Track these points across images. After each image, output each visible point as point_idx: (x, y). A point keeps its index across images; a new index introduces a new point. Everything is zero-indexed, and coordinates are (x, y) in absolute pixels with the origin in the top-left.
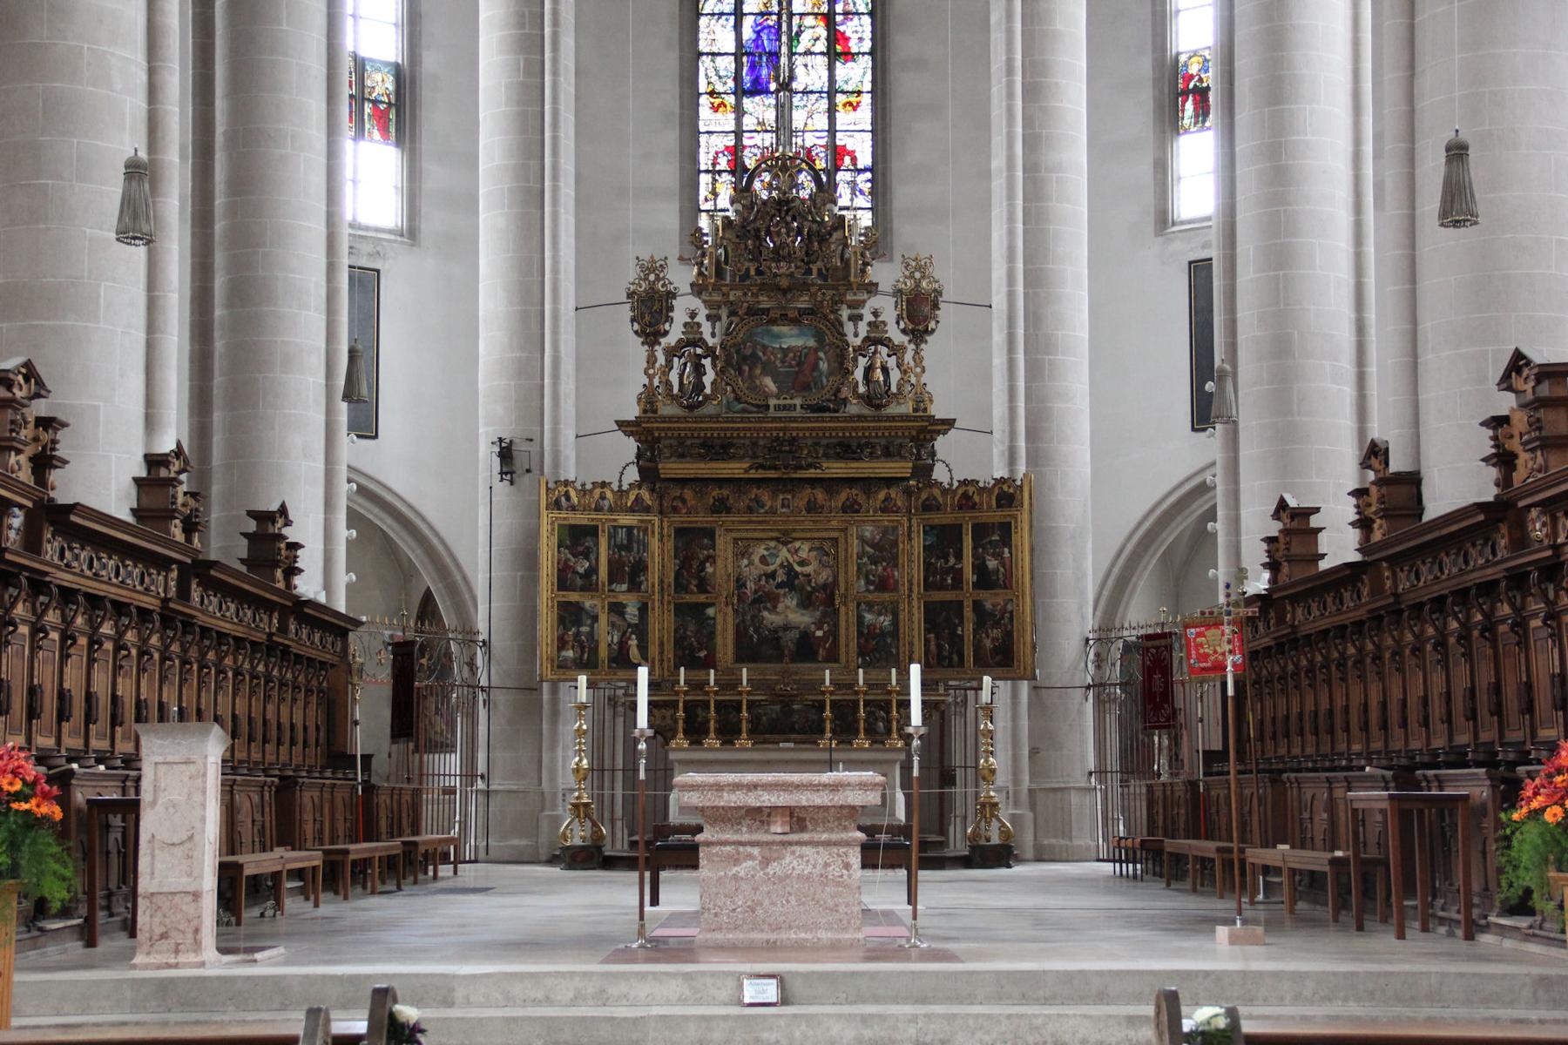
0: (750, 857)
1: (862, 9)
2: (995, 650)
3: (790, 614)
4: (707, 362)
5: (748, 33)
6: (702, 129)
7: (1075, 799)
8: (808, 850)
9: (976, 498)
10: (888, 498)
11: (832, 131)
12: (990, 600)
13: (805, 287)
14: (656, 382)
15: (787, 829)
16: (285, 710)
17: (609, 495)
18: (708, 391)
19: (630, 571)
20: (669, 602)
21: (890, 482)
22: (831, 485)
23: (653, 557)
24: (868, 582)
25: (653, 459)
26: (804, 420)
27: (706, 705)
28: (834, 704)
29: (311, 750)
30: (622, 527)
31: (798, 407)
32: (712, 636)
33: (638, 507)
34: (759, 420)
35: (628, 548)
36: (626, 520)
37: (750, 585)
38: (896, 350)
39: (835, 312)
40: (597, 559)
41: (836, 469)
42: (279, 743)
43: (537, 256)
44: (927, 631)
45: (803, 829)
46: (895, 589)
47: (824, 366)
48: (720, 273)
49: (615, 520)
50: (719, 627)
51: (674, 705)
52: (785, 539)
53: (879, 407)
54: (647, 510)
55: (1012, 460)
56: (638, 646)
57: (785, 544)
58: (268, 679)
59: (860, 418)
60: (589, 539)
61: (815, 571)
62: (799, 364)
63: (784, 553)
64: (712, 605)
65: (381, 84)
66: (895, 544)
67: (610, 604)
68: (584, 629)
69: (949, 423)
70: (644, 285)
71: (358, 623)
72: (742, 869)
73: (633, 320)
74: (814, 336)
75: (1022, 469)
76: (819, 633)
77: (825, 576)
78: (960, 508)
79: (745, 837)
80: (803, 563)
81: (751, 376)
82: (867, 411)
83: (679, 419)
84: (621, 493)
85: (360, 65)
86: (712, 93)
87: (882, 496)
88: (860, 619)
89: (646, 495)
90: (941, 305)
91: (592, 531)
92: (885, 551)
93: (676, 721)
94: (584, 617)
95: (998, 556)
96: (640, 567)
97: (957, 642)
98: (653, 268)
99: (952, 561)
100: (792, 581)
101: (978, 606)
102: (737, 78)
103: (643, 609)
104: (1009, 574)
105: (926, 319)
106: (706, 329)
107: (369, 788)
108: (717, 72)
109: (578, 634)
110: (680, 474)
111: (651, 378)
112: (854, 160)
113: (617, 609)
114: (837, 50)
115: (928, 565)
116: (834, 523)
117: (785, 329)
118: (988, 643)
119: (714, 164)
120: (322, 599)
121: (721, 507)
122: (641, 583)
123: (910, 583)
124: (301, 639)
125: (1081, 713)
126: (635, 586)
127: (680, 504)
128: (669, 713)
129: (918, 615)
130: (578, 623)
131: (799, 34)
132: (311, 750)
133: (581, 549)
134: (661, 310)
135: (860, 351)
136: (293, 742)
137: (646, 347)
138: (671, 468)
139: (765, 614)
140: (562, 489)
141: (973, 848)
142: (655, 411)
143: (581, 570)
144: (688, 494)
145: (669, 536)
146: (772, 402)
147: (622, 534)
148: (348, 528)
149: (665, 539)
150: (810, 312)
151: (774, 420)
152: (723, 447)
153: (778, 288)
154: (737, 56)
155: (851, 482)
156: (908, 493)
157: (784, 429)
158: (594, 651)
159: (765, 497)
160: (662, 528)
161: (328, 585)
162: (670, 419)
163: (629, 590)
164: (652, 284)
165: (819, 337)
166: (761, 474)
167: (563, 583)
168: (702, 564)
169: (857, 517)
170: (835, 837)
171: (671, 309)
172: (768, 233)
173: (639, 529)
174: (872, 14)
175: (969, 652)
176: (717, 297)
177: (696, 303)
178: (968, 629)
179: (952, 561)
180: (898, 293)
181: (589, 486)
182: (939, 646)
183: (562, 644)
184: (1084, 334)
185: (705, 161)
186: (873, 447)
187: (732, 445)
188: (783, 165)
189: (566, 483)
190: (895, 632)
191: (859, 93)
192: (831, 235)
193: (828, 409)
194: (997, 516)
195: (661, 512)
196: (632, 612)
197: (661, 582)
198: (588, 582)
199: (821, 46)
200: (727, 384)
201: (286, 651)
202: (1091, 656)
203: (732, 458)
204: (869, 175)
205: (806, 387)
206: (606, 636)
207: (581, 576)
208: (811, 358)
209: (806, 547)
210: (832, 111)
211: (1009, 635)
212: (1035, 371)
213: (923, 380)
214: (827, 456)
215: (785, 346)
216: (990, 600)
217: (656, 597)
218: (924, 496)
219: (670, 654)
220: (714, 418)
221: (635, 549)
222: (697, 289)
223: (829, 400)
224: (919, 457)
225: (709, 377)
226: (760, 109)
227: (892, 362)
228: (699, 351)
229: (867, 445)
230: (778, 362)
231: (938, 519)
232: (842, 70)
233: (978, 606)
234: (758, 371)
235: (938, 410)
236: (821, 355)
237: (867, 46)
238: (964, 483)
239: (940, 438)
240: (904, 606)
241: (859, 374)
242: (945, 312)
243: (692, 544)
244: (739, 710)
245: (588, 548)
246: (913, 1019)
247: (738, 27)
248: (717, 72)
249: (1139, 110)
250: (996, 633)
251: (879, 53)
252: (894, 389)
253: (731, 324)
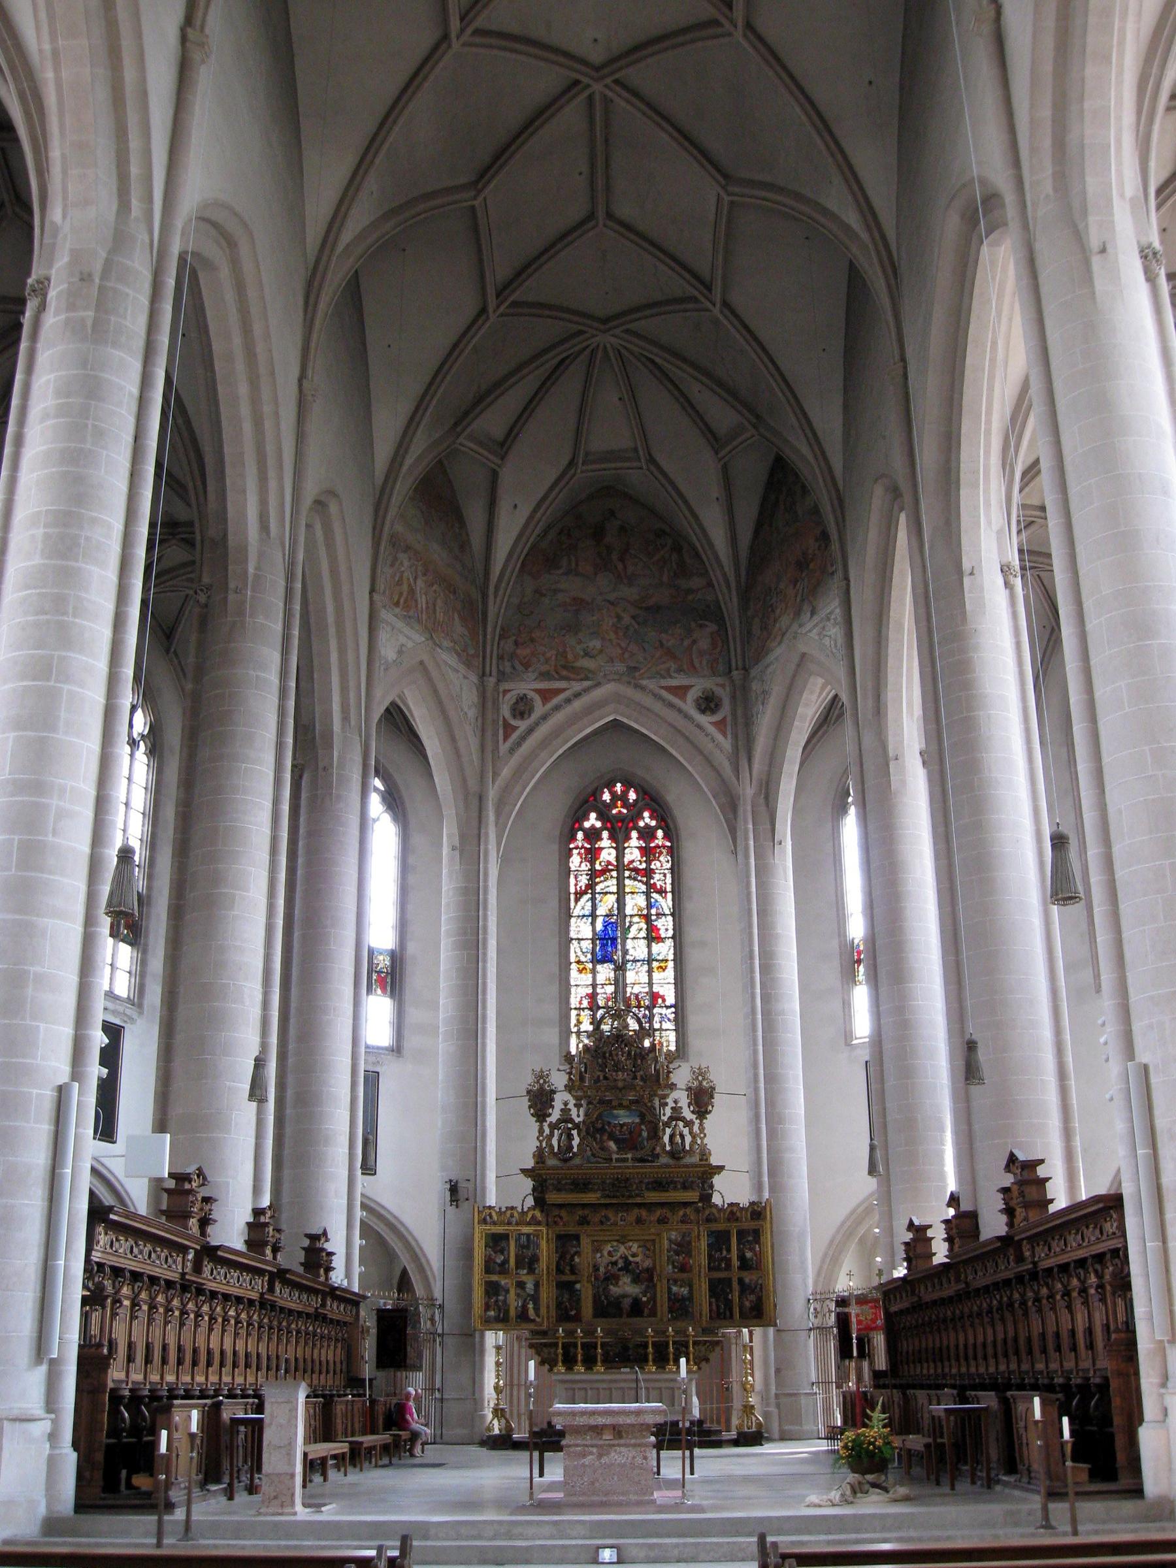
0: (591, 1453)
1: (667, 912)
2: (752, 1309)
3: (626, 1287)
4: (575, 1132)
5: (599, 926)
6: (573, 982)
7: (803, 1401)
8: (623, 1449)
9: (738, 1214)
10: (685, 1215)
11: (650, 984)
12: (748, 1277)
13: (632, 1087)
14: (544, 1145)
15: (611, 1437)
16: (323, 1352)
17: (516, 1214)
18: (575, 1150)
19: (529, 1262)
21: (686, 1204)
22: (650, 1207)
24: (674, 1267)
25: (542, 1192)
26: (634, 1167)
27: (575, 1346)
28: (654, 1344)
29: (338, 1377)
32: (579, 1300)
33: (534, 1222)
34: (608, 1168)
35: (527, 1247)
36: (526, 1230)
37: (602, 1270)
38: (689, 1124)
39: (651, 1101)
41: (653, 1197)
42: (320, 1373)
43: (472, 1069)
44: (710, 1297)
45: (621, 1437)
46: (690, 1271)
47: (645, 1134)
48: (582, 1079)
50: (583, 1297)
51: (556, 1345)
52: (623, 1240)
53: (678, 1159)
54: (539, 1223)
55: (759, 1187)
57: (623, 1243)
58: (315, 1335)
59: (667, 1166)
61: (641, 1260)
62: (631, 1133)
63: (622, 1250)
64: (578, 1282)
65: (383, 962)
66: (690, 1243)
68: (501, 1298)
69: (721, 1168)
70: (537, 1086)
71: (364, 1297)
72: (587, 1460)
73: (530, 1107)
75: (766, 1195)
76: (644, 1299)
77: (648, 1263)
78: (729, 1220)
79: (589, 1442)
80: (634, 1255)
81: (602, 1141)
82: (671, 1162)
83: (557, 1168)
84: (523, 1213)
85: (371, 952)
86: (578, 962)
87: (681, 1213)
88: (669, 1289)
89: (538, 1214)
90: (716, 1095)
91: (505, 1237)
92: (683, 1247)
93: (557, 1355)
95: (751, 1249)
96: (535, 1259)
97: (729, 1304)
98: (541, 1076)
99: (725, 1253)
100: (627, 1267)
101: (741, 1281)
102: (593, 953)
103: (537, 1285)
104: (759, 1262)
105: (707, 1105)
106: (574, 1112)
107: (373, 1402)
108: (580, 950)
109: (497, 1301)
110: (559, 1201)
111: (541, 1142)
112: (664, 1000)
113: (521, 1285)
114: (653, 936)
115: (710, 1256)
116: (653, 1230)
117: (621, 1112)
118: (747, 1304)
119: (580, 1003)
120: (345, 1283)
121: (584, 1221)
123: (700, 1266)
124: (334, 1309)
125: (806, 1346)
126: (531, 1271)
128: (552, 1350)
129: (705, 1286)
130: (497, 1294)
131: (629, 927)
132: (338, 1377)
135: (667, 1124)
136: (328, 1372)
138: (553, 1197)
139: (611, 1287)
140: (487, 1211)
141: (739, 1434)
142: (543, 1163)
143: (499, 1261)
144: (563, 1213)
146: (615, 1156)
147: (524, 1239)
148: (361, 1238)
150: (637, 1102)
151: (615, 1167)
153: (616, 1087)
154: (593, 940)
155: (662, 1205)
156: (697, 1211)
157: (622, 1174)
158: (507, 1312)
159: (611, 1215)
161: (348, 1275)
162: (553, 1168)
163: (528, 1273)
164: (542, 1088)
165: (642, 1116)
166: (608, 1201)
167: (488, 1270)
168: (572, 1259)
169: (668, 1226)
170: (638, 1441)
171: (553, 1100)
172: (611, 1055)
174: (672, 915)
175: (736, 1310)
176: (580, 1093)
177: (567, 1096)
178: (735, 1296)
179: (725, 1253)
180: (689, 1089)
181: (503, 1209)
182: (718, 1307)
183: (487, 1307)
184: (801, 1111)
185: (574, 1002)
187: (589, 1183)
188: (621, 1005)
189: (490, 1207)
190: (690, 1298)
191: (667, 961)
193: (648, 1161)
194: (752, 1225)
196: (530, 1286)
197: (548, 1268)
198: (503, 1269)
199: (643, 934)
201: (325, 1317)
202: (812, 1310)
203: (592, 1190)
204: (673, 1010)
205: (634, 1148)
206: (514, 1302)
207: (500, 1265)
209: (635, 1246)
210: (650, 972)
211: (760, 1299)
212: (772, 1134)
213: (705, 1141)
214: (648, 1189)
216: (748, 1277)
218: (707, 1212)
219: (553, 1313)
220: (579, 1167)
222: (569, 1088)
224: (703, 1189)
225: (576, 1142)
226: (605, 972)
227: (686, 1131)
228: (570, 1126)
229: (672, 1182)
231: (715, 1227)
232: (656, 948)
233: (741, 1281)
234: (605, 1138)
235: (714, 1161)
237: (670, 933)
238: (731, 1205)
239: (716, 1177)
240: (696, 1281)
241: (666, 1139)
242: (717, 1099)
243: (565, 1242)
244: (596, 1348)
246: (677, 1545)
247: (593, 924)
248: (580, 950)
249: (831, 973)
250: (752, 1297)
251: (677, 937)
252: (687, 1148)
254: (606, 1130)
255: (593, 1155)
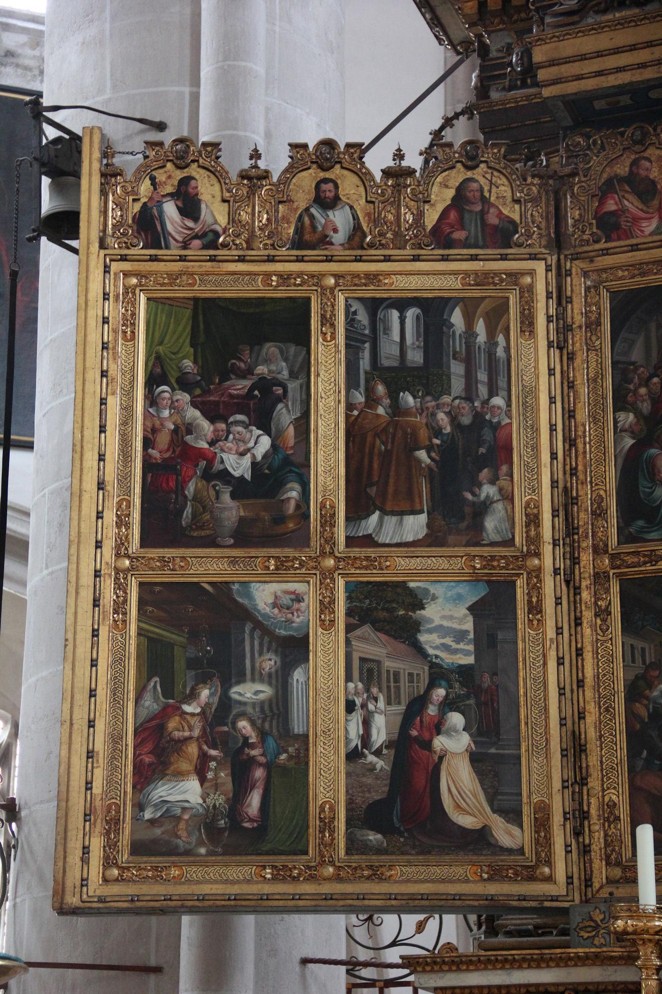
17: (349, 186)
20: (600, 578)
23: (530, 408)
30: (402, 305)
40: (303, 424)
49: (373, 278)
56: (475, 759)
60: (271, 349)
67: (353, 591)
94: (250, 642)
122: (482, 509)
127: (632, 204)
133: (240, 386)
145: (593, 325)
149: (577, 341)
160: (561, 298)
173: (470, 308)
195: (558, 242)
217: (548, 558)
221: (458, 385)
245: (265, 385)
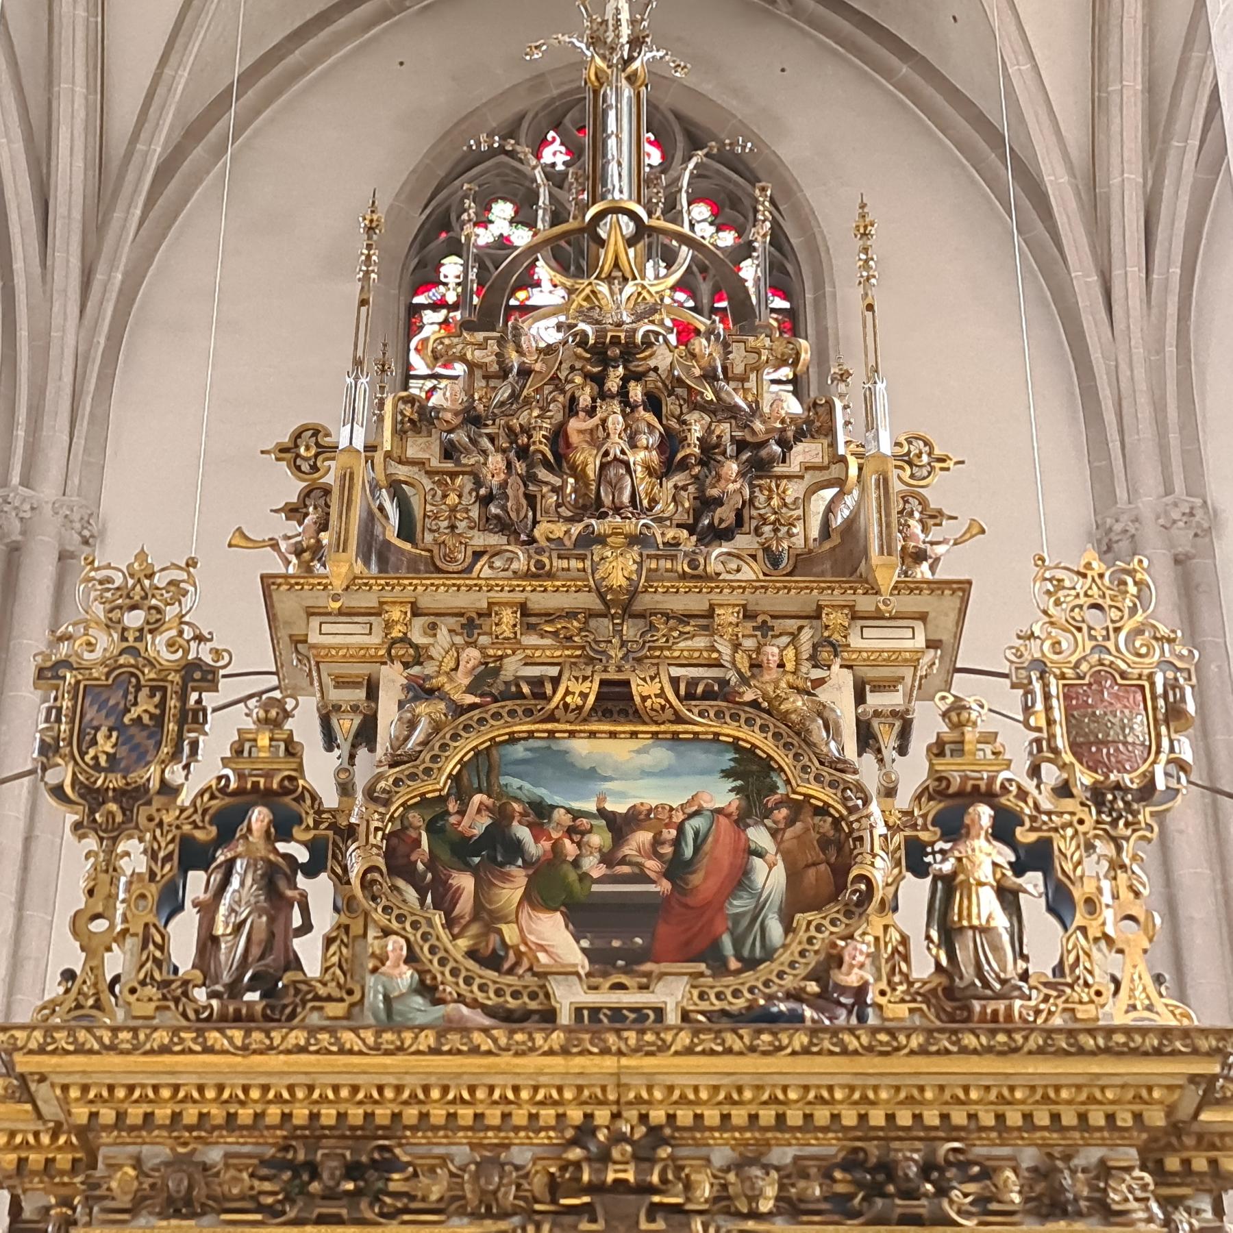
31: (672, 1018)
62: (677, 868)
70: (105, 643)
74: (727, 774)
134: (159, 720)
137: (91, 843)
152: (353, 1170)
171: (194, 717)
186: (987, 1174)
192: (786, 445)
200: (387, 933)
208: (721, 850)
215: (618, 807)
223: (796, 996)
230: (592, 866)
234: (511, 892)
236: (759, 836)
253: (412, 725)
254: (515, 849)
255: (427, 989)
